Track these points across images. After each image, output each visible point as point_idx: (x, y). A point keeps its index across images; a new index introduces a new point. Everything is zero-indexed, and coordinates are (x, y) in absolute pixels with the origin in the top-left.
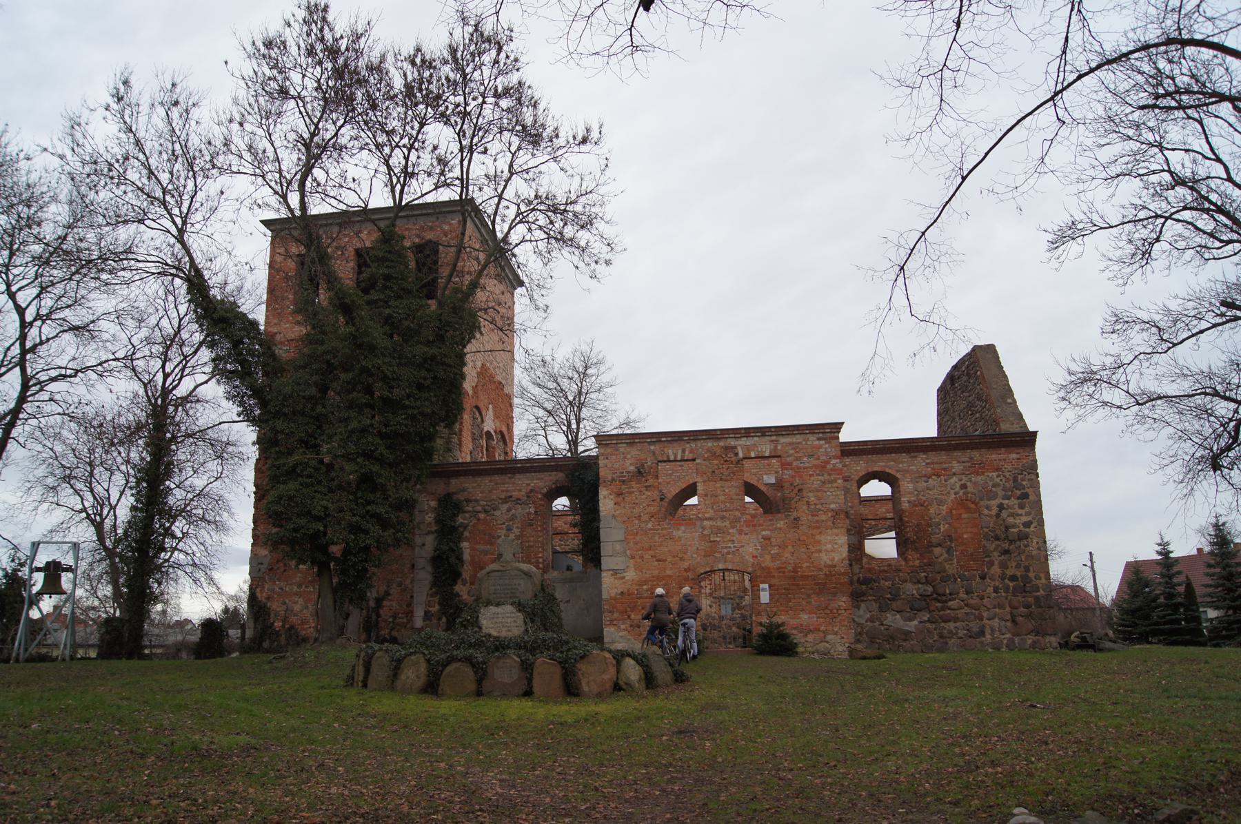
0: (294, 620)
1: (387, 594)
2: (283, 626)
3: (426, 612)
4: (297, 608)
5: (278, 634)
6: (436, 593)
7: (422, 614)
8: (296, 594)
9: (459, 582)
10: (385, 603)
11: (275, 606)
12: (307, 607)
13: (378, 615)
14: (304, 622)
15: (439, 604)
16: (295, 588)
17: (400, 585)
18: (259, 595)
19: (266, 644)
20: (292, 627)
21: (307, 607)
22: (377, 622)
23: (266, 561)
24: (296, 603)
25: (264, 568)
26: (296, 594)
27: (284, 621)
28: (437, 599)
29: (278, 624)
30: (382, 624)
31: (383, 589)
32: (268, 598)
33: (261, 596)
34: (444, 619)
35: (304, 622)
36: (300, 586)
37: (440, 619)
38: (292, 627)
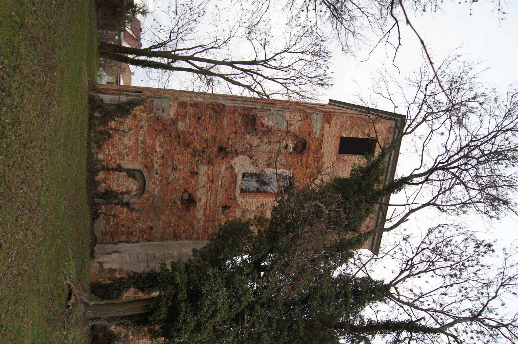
0: (116, 138)
1: (132, 210)
2: (111, 129)
3: (115, 270)
4: (126, 140)
5: (105, 124)
6: (129, 275)
7: (114, 267)
8: (137, 139)
9: (137, 290)
10: (125, 209)
11: (129, 121)
12: (125, 148)
13: (116, 204)
14: (114, 146)
15: (121, 279)
16: (141, 139)
17: (138, 219)
18: (138, 108)
19: (97, 114)
20: (110, 136)
21: (125, 148)
22: (110, 203)
23: (165, 115)
24: (130, 140)
25: (160, 113)
26: (137, 139)
27: (116, 130)
28: (125, 276)
29: (113, 124)
30: (109, 207)
31: (137, 207)
32: (135, 116)
33: (136, 110)
34: (109, 282)
35: (114, 146)
36: (143, 142)
37: (109, 279)
38: (110, 136)
